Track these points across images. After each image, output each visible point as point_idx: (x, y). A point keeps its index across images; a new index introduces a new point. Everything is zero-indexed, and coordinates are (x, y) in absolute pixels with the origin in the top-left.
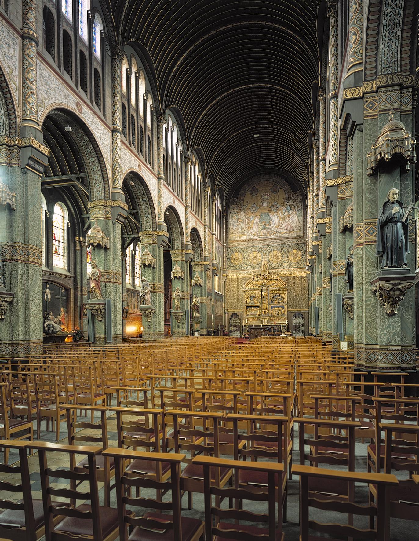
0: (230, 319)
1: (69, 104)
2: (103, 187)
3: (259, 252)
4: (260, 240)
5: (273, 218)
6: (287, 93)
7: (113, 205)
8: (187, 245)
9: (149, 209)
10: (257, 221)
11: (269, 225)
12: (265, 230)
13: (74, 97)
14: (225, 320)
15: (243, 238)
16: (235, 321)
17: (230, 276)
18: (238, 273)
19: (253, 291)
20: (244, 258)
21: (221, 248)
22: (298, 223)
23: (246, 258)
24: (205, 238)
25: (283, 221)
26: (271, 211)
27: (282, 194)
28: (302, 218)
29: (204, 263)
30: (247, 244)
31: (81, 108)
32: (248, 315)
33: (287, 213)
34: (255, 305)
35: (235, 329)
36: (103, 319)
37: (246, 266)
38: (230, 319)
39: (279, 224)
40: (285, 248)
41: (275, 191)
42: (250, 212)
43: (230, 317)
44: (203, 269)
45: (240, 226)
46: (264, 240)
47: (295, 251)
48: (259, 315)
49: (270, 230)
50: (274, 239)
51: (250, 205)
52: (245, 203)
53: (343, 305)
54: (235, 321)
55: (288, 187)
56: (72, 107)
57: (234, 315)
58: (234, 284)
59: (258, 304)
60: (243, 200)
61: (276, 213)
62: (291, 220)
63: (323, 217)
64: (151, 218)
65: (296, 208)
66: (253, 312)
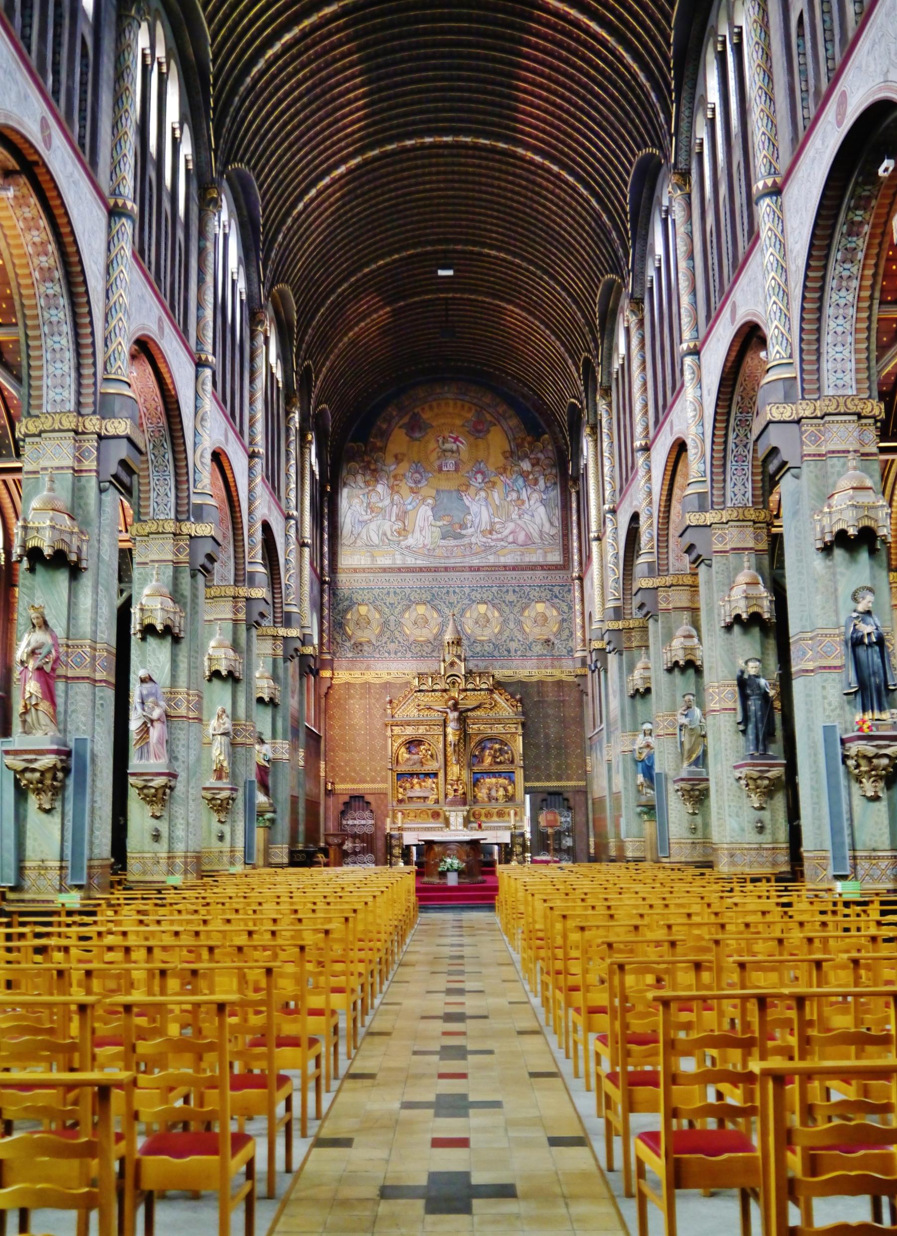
0: (343, 813)
1: (26, 119)
2: (73, 374)
4: (436, 570)
5: (474, 508)
6: (549, 171)
7: (103, 432)
8: (252, 575)
9: (169, 456)
10: (425, 512)
11: (463, 526)
12: (453, 542)
13: (38, 101)
15: (384, 561)
16: (360, 822)
17: (342, 676)
18: (368, 668)
19: (418, 723)
20: (385, 624)
21: (316, 588)
22: (547, 525)
23: (392, 623)
24: (287, 553)
25: (510, 515)
26: (468, 486)
27: (497, 441)
28: (558, 512)
29: (282, 632)
30: (395, 580)
31: (50, 136)
32: (400, 801)
33: (514, 495)
35: (359, 846)
36: (58, 805)
37: (392, 647)
38: (343, 813)
39: (492, 524)
40: (511, 597)
41: (478, 431)
42: (405, 487)
43: (341, 808)
44: (280, 652)
45: (373, 526)
46: (446, 569)
47: (540, 607)
48: (437, 801)
49: (466, 541)
50: (479, 569)
51: (404, 465)
52: (390, 459)
53: (845, 758)
54: (360, 822)
55: (514, 422)
56: (32, 130)
57: (357, 801)
58: (356, 707)
60: (383, 449)
61: (483, 494)
62: (526, 516)
63: (702, 509)
64: (172, 483)
65: (541, 482)
66: (417, 792)
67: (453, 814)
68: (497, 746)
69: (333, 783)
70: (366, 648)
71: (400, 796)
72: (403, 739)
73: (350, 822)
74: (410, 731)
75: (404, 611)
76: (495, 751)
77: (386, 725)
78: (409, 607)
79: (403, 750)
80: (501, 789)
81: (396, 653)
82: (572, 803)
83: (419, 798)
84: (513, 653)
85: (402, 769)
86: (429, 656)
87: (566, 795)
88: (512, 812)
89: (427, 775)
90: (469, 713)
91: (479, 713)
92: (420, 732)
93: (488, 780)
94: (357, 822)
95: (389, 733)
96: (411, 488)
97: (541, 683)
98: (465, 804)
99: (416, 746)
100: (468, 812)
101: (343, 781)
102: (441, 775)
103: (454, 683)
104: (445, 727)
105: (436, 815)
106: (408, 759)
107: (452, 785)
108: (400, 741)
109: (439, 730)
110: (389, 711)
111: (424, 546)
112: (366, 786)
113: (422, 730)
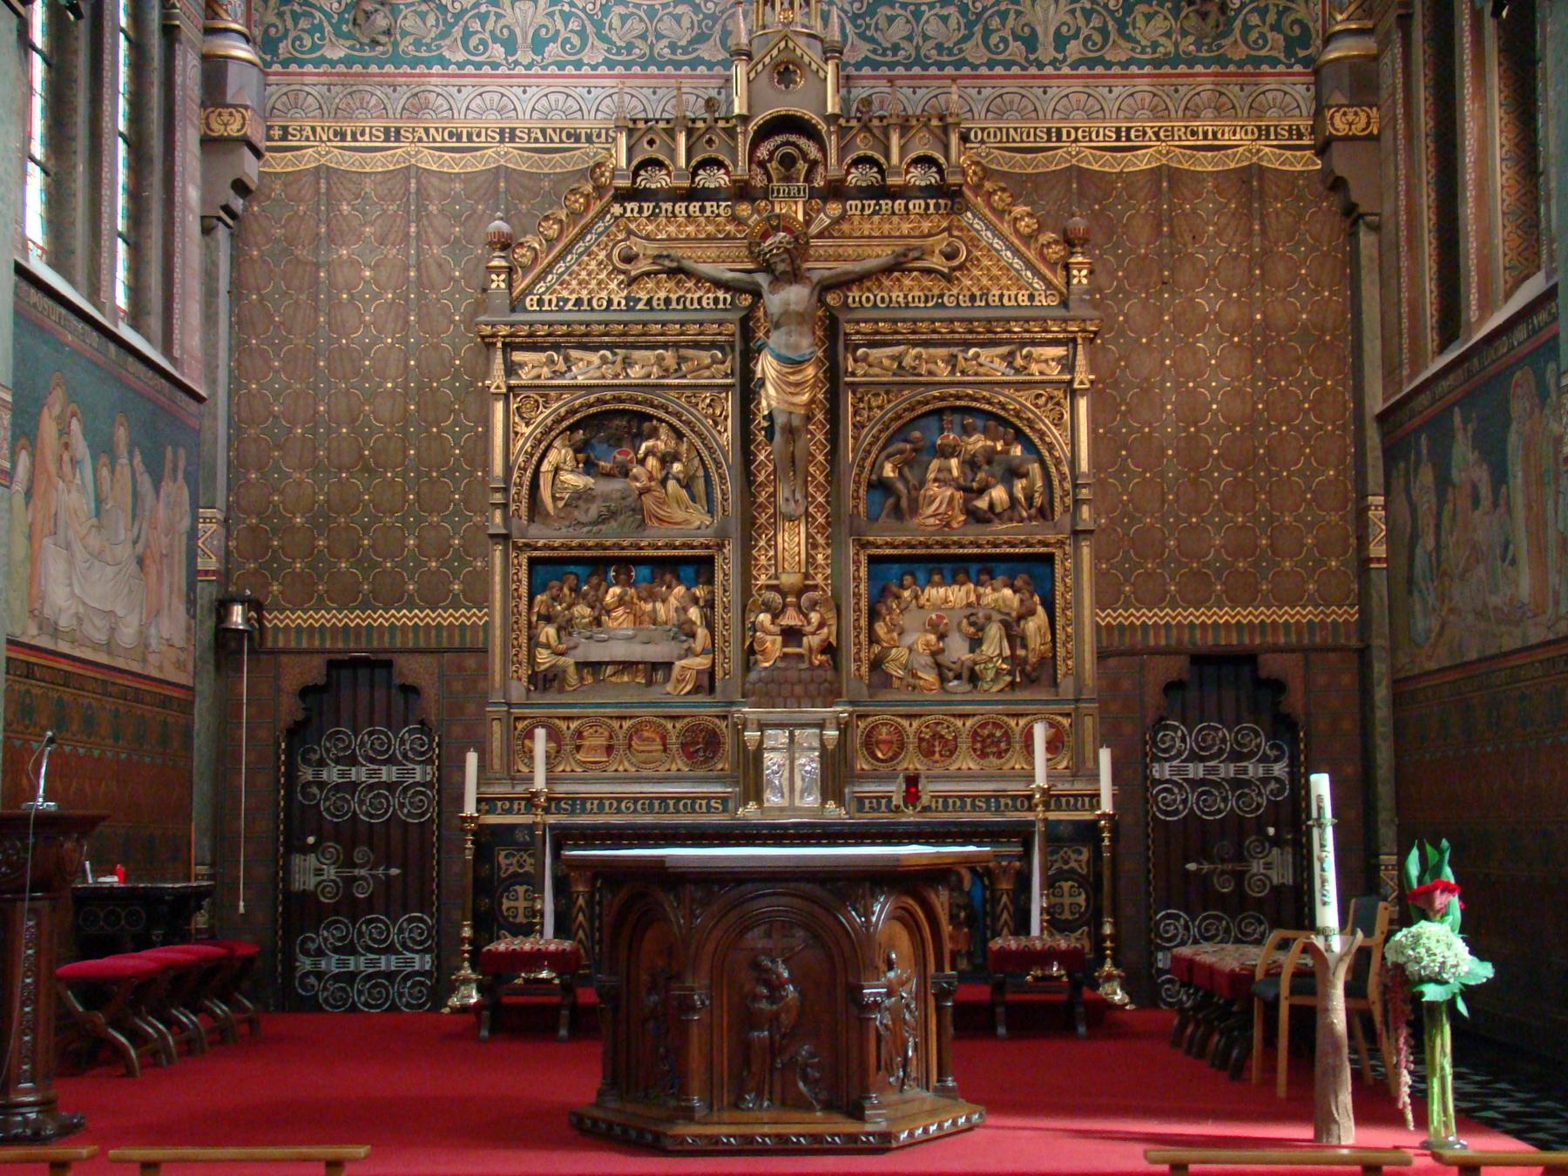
14: (225, 757)
16: (365, 772)
32: (545, 681)
34: (654, 540)
43: (289, 709)
48: (707, 682)
54: (365, 772)
66: (620, 639)
67: (779, 737)
68: (977, 443)
69: (255, 605)
70: (409, 22)
71: (544, 658)
72: (557, 406)
73: (332, 774)
74: (587, 368)
76: (971, 464)
77: (488, 344)
79: (560, 454)
80: (994, 631)
81: (538, 45)
82: (1295, 701)
83: (626, 666)
84: (1046, 52)
85: (549, 536)
86: (685, 59)
87: (1271, 666)
88: (1040, 733)
89: (667, 567)
90: (854, 293)
91: (905, 291)
92: (636, 372)
93: (936, 593)
94: (359, 774)
95: (497, 380)
97: (1167, 179)
98: (832, 695)
99: (615, 442)
100: (844, 728)
101: (304, 598)
102: (727, 566)
103: (788, 162)
104: (749, 356)
105: (702, 745)
106: (581, 496)
108: (544, 415)
109: (716, 369)
110: (498, 282)
112: (404, 617)
113: (642, 368)
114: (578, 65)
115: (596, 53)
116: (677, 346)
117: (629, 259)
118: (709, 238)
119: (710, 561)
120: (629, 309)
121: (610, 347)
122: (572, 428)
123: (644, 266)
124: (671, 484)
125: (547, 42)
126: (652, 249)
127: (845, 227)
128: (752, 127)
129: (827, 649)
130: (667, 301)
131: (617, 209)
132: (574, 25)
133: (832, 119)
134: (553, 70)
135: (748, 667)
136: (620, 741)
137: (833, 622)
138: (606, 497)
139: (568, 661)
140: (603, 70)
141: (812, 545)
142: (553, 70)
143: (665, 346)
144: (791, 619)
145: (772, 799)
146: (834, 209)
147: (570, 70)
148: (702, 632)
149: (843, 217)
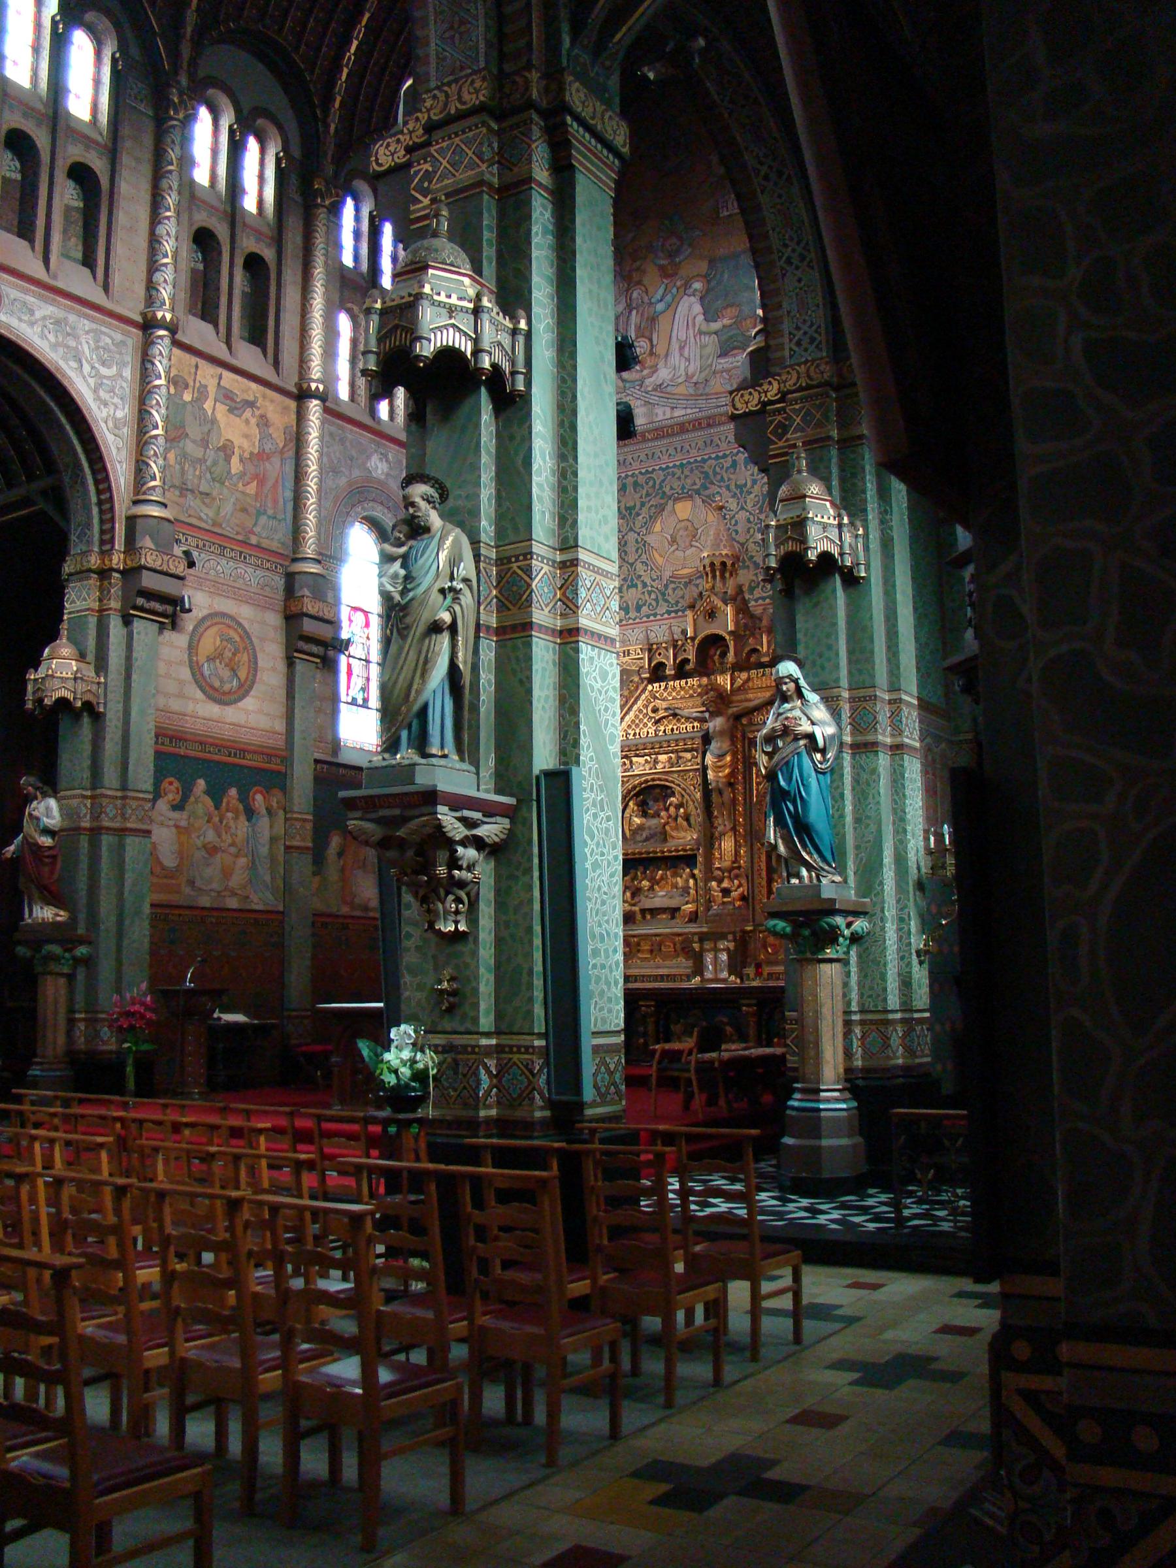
3: (707, 501)
10: (690, 307)
59: (685, 838)
75: (652, 519)
78: (661, 509)
81: (638, 608)
96: (662, 268)
99: (656, 800)
106: (641, 828)
107: (720, 881)
111: (688, 377)
114: (655, 615)
115: (663, 608)
116: (677, 751)
117: (655, 710)
118: (691, 696)
119: (695, 856)
120: (656, 735)
121: (649, 755)
122: (637, 795)
123: (661, 714)
124: (679, 819)
125: (641, 607)
126: (664, 705)
127: (750, 684)
128: (697, 642)
129: (743, 898)
130: (672, 730)
131: (650, 687)
132: (653, 596)
133: (731, 633)
134: (645, 619)
135: (708, 909)
136: (656, 947)
137: (745, 884)
138: (650, 828)
139: (636, 909)
140: (666, 616)
141: (737, 846)
142: (645, 619)
143: (672, 752)
144: (725, 884)
145: (708, 975)
146: (744, 675)
147: (652, 618)
148: (692, 892)
149: (749, 679)
